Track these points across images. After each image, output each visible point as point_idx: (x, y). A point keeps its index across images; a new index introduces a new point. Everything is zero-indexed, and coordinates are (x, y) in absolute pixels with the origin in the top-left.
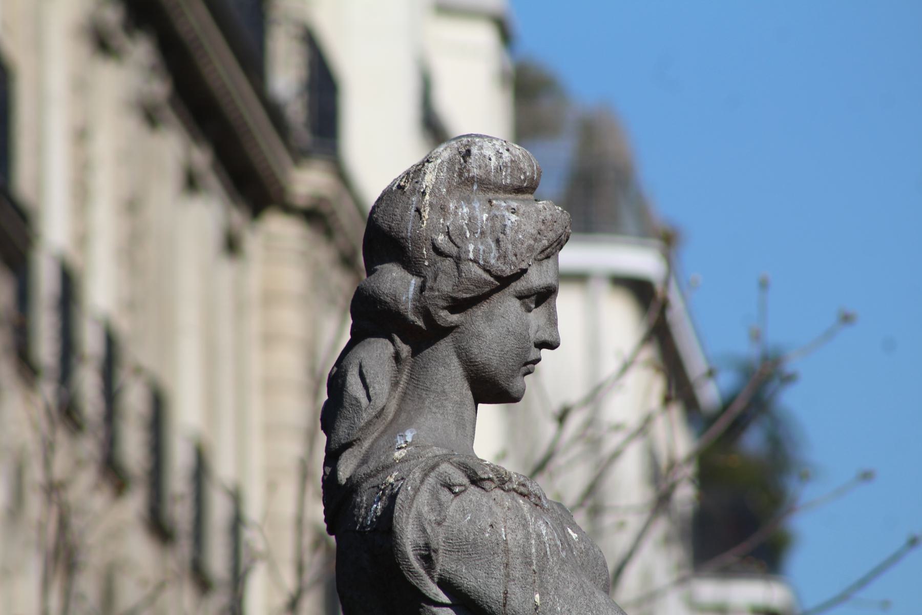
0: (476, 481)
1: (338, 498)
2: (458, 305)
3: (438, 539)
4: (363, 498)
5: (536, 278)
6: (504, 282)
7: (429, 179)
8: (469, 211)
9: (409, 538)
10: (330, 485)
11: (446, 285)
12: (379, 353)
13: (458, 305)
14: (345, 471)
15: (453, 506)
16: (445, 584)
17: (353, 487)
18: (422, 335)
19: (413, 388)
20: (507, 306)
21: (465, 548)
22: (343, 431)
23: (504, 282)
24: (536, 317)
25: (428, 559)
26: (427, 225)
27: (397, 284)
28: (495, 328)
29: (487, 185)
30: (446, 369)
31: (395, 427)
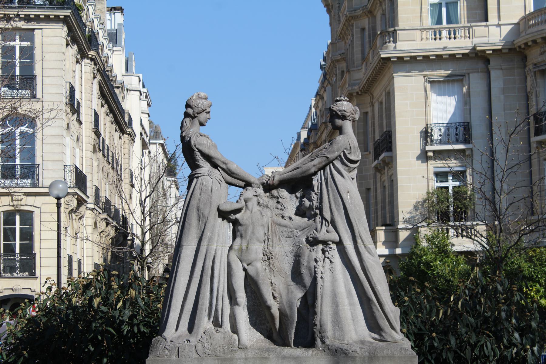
0: (201, 135)
1: (183, 138)
2: (198, 113)
3: (196, 143)
4: (186, 138)
5: (208, 110)
6: (204, 110)
7: (194, 97)
8: (199, 101)
9: (193, 143)
10: (181, 136)
11: (196, 111)
12: (188, 120)
13: (198, 113)
14: (183, 135)
15: (198, 139)
16: (197, 149)
17: (185, 136)
18: (193, 117)
19: (192, 124)
20: (204, 113)
21: (199, 144)
22: (183, 130)
23: (204, 110)
24: (208, 115)
25: (195, 145)
26: (193, 103)
27: (190, 111)
28: (203, 117)
29: (201, 98)
30: (196, 121)
31: (190, 129)
